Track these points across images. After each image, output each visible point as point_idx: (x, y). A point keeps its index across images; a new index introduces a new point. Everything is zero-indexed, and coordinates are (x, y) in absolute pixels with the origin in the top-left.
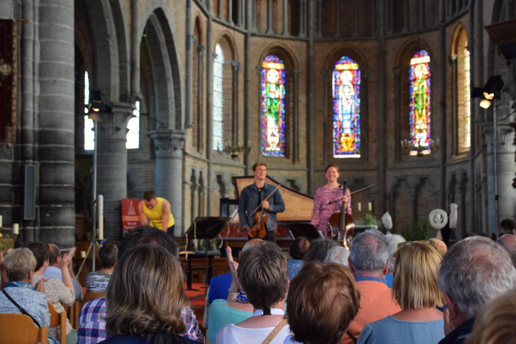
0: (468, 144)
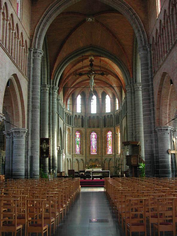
0: (120, 152)
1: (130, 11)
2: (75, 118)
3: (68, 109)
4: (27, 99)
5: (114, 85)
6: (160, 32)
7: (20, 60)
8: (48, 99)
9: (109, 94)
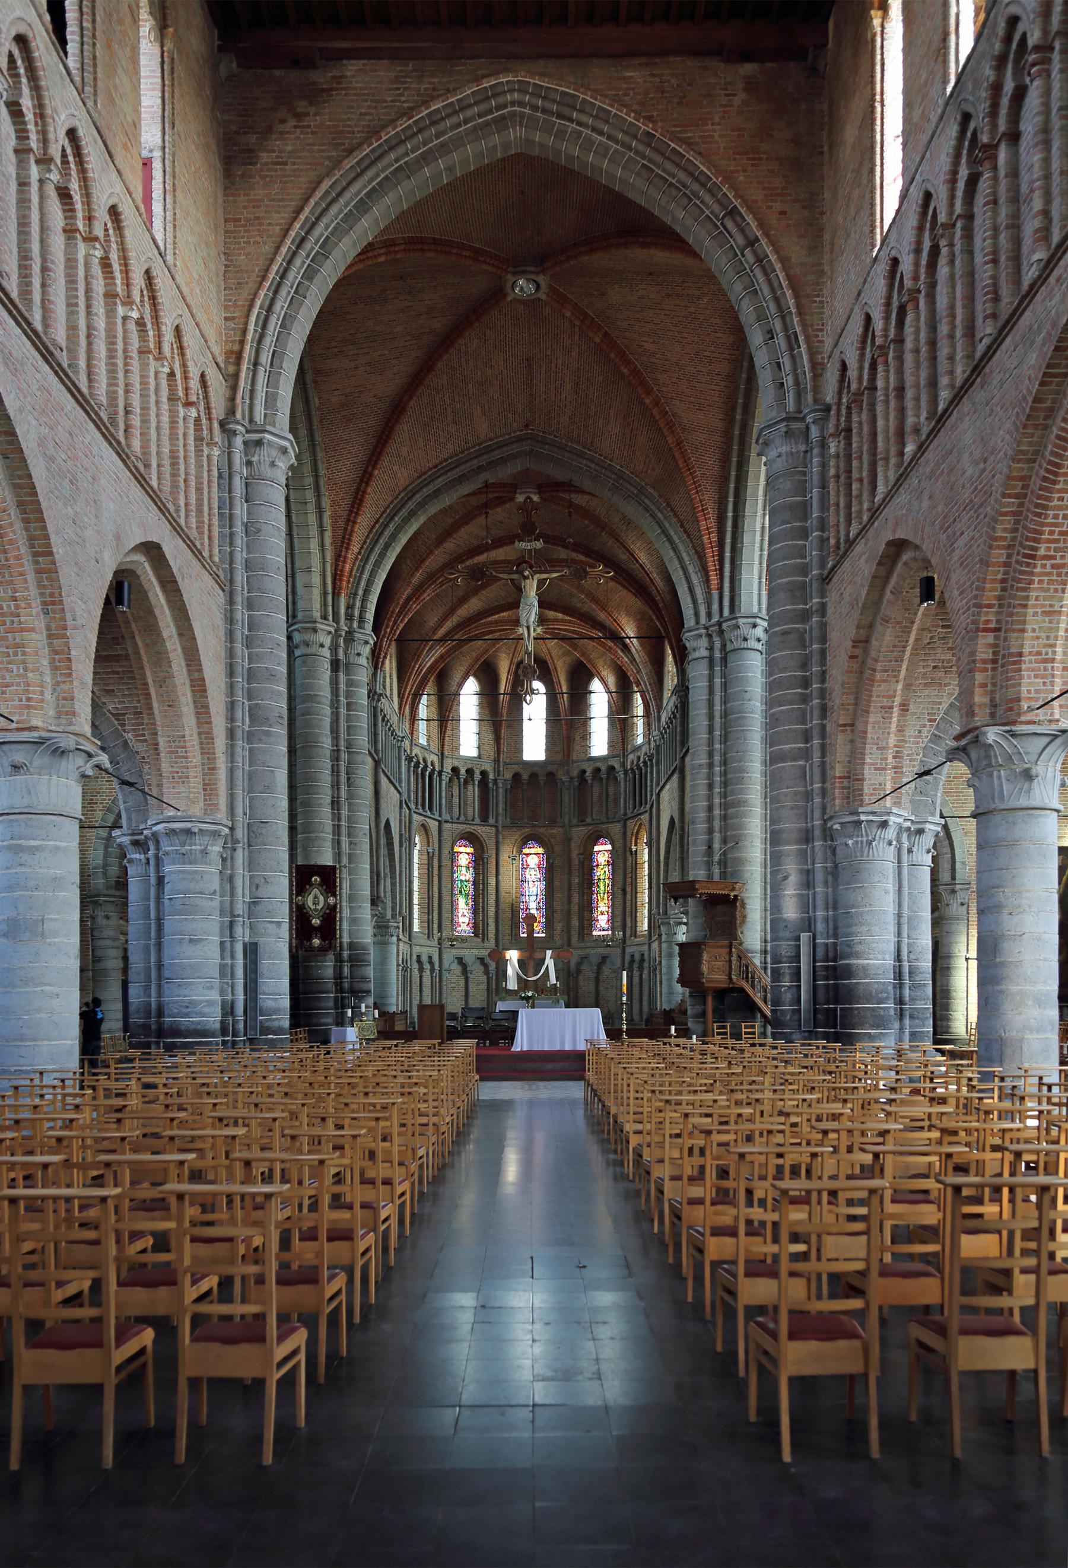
1: (729, 224)
2: (451, 780)
3: (423, 741)
4: (223, 676)
5: (629, 630)
6: (886, 330)
7: (174, 475)
8: (329, 690)
9: (604, 673)
